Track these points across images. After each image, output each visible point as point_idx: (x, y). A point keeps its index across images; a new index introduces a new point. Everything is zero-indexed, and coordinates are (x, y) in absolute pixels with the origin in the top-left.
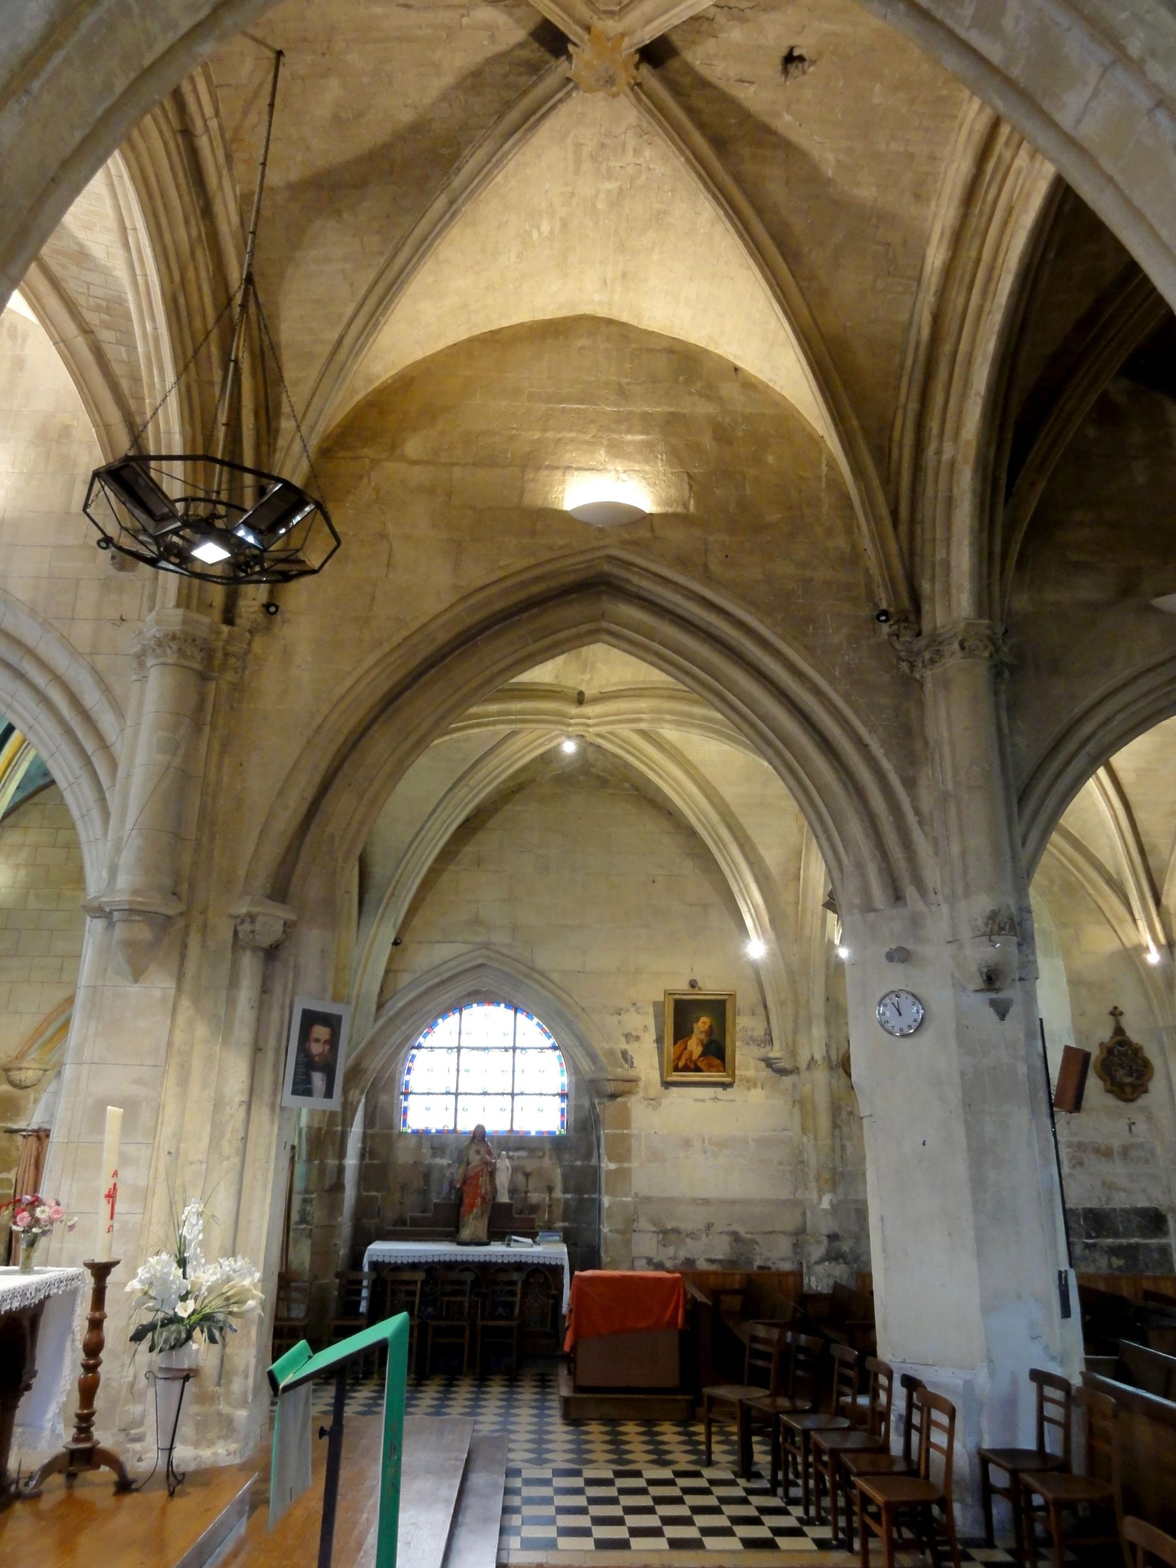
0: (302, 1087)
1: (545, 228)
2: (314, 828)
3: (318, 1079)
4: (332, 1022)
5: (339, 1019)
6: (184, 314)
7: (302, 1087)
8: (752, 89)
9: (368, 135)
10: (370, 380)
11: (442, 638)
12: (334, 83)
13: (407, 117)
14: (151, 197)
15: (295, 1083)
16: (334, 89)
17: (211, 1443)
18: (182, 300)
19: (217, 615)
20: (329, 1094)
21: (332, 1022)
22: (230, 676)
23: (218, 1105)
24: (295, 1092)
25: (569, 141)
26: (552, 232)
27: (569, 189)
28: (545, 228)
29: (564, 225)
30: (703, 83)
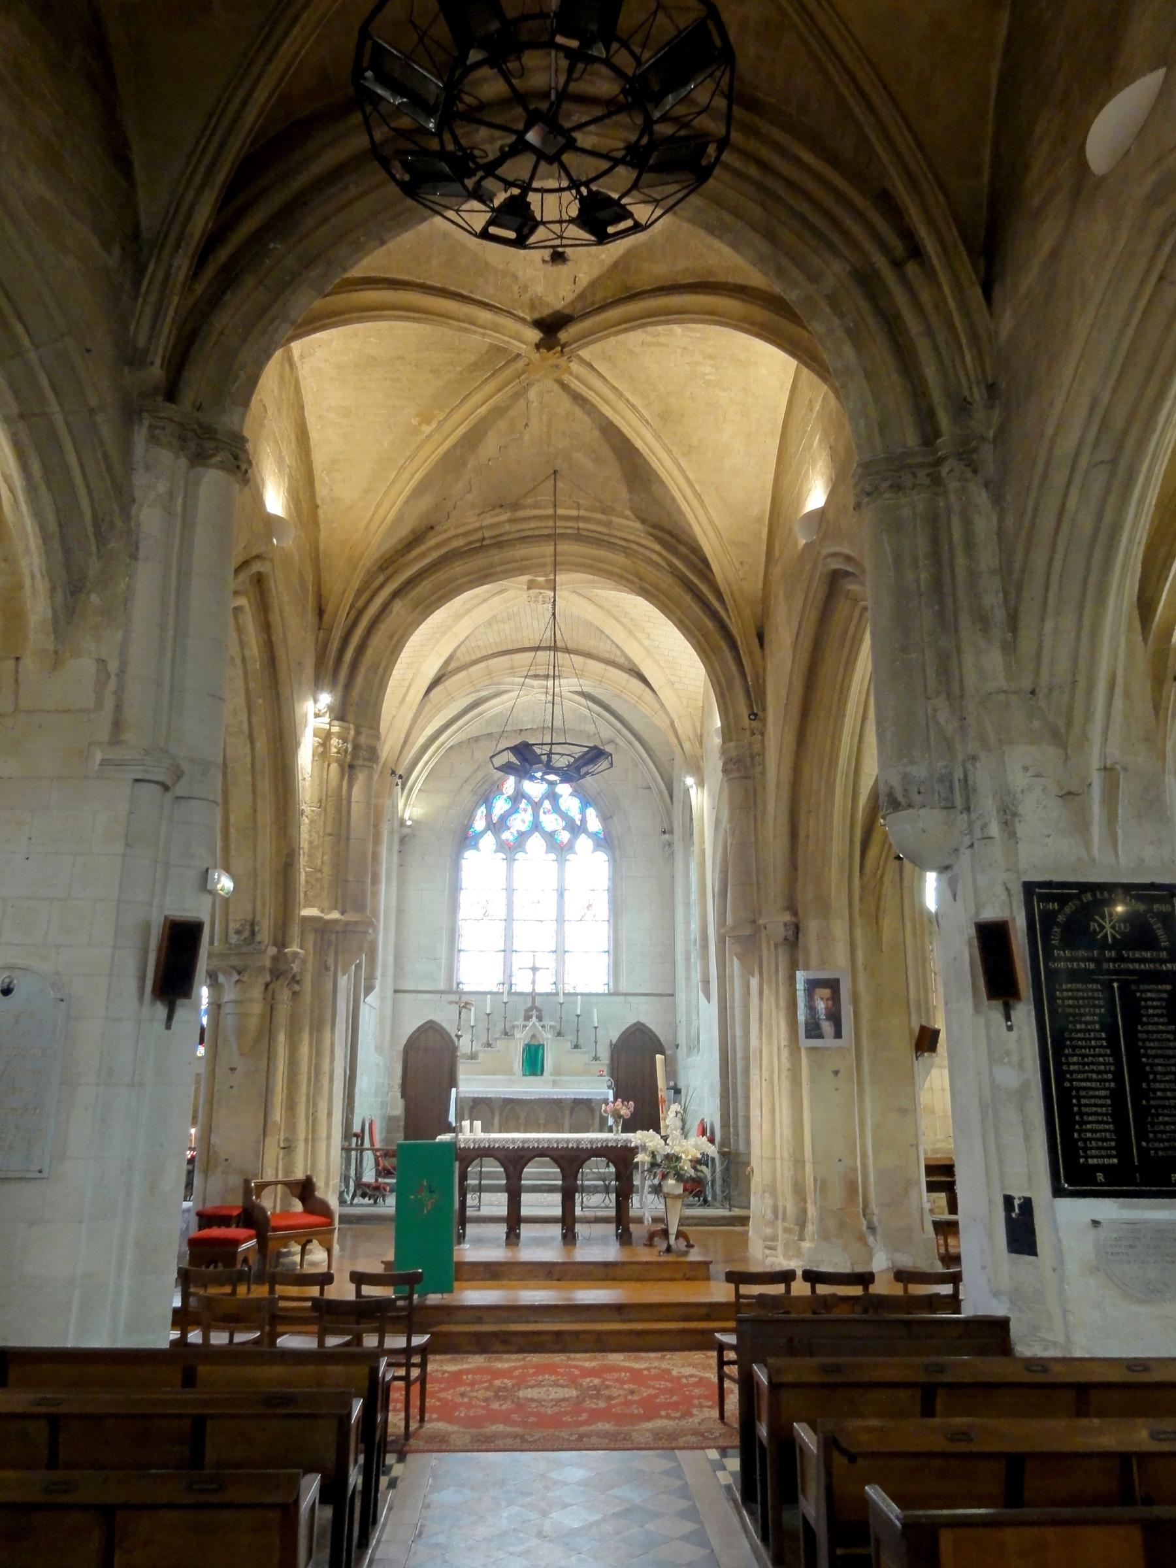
0: (814, 1031)
1: (708, 370)
2: (800, 853)
3: (827, 1027)
4: (833, 985)
5: (837, 981)
6: (652, 589)
7: (813, 1033)
8: (581, 275)
9: (606, 451)
10: (760, 519)
11: (798, 687)
12: (575, 455)
13: (597, 433)
14: (591, 567)
15: (807, 1031)
16: (579, 457)
17: (790, 1259)
18: (647, 586)
19: (748, 733)
20: (838, 1034)
21: (833, 985)
22: (759, 769)
23: (779, 1049)
24: (807, 1037)
25: (637, 350)
26: (711, 366)
27: (679, 350)
28: (708, 370)
29: (710, 357)
30: (582, 296)
